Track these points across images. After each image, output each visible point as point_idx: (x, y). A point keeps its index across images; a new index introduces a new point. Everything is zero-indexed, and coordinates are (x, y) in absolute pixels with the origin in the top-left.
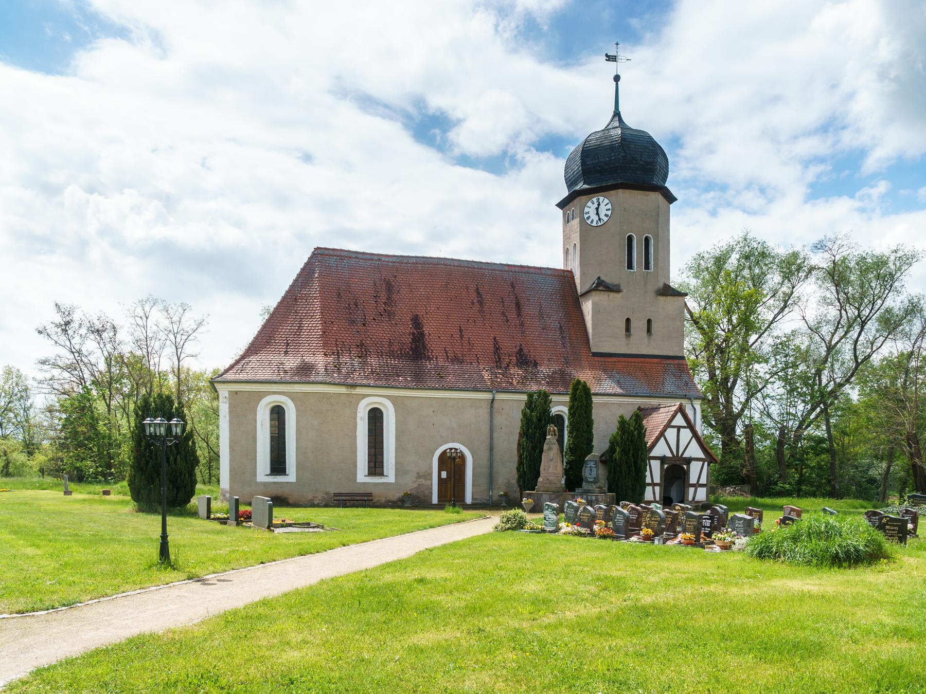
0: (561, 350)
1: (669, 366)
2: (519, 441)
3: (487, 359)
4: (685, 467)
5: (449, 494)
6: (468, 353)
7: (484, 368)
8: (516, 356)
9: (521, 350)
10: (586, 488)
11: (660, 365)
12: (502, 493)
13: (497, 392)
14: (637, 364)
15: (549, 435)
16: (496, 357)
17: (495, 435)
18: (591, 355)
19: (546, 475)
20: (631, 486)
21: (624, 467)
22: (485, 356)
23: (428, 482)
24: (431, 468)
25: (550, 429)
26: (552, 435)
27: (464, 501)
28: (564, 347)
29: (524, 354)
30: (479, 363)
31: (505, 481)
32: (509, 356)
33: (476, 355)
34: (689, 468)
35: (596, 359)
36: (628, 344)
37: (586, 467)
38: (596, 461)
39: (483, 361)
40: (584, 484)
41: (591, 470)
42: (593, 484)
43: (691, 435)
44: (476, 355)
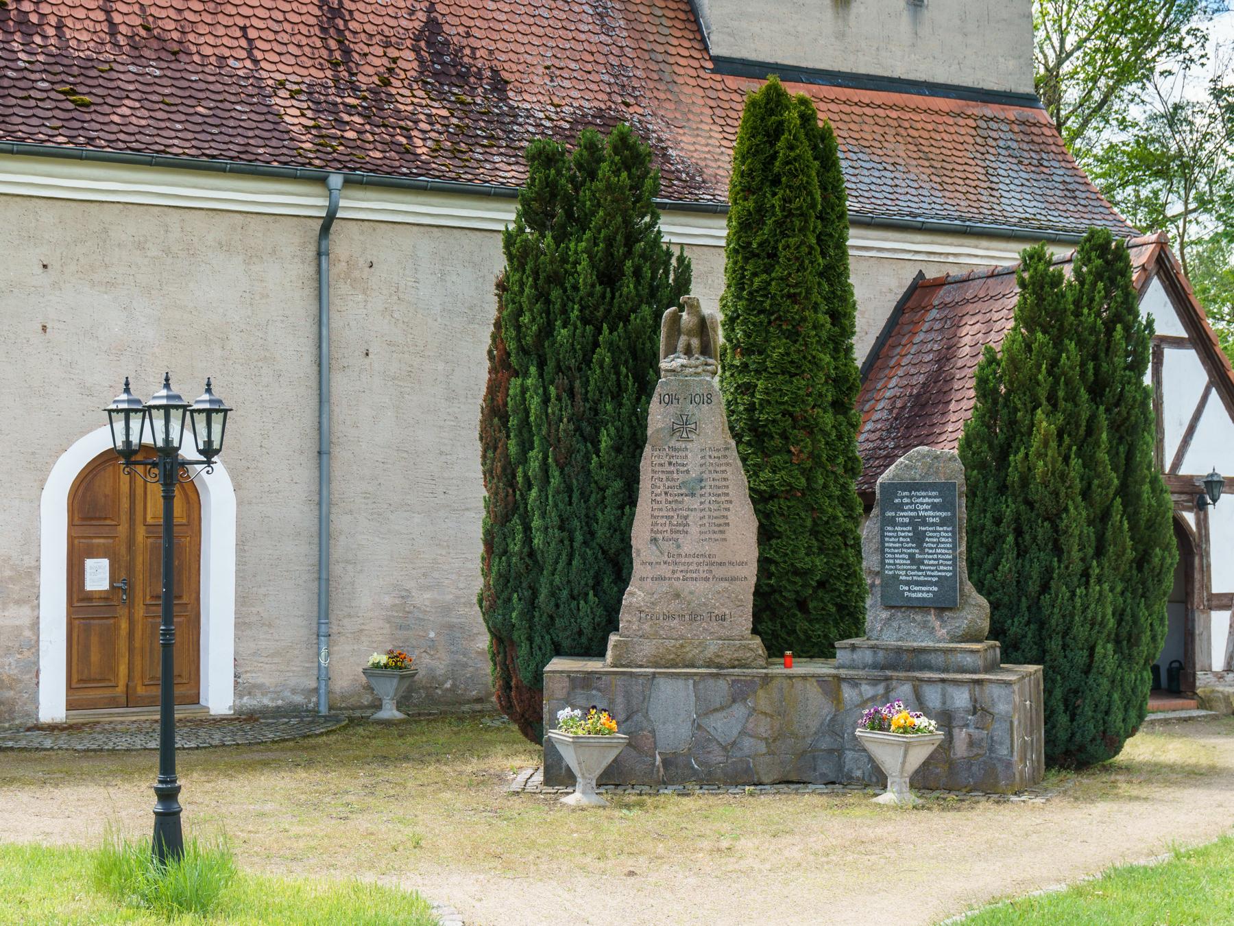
0: (594, 39)
1: (993, 125)
2: (494, 389)
3: (292, 49)
4: (1190, 518)
5: (123, 669)
6: (208, 18)
7: (282, 84)
8: (416, 50)
9: (433, 25)
10: (890, 639)
11: (961, 121)
12: (383, 659)
13: (348, 182)
14: (881, 112)
15: (671, 350)
16: (333, 44)
17: (340, 384)
18: (709, 65)
19: (665, 570)
20: (1111, 623)
21: (1077, 519)
22: (284, 38)
23: (17, 616)
24: (31, 540)
25: (676, 319)
26: (688, 352)
27: (199, 703)
28: (607, 30)
29: (446, 43)
30: (256, 61)
31: (388, 600)
32: (387, 45)
33: (244, 29)
34: (1203, 523)
35: (732, 82)
36: (841, 36)
37: (892, 522)
38: (945, 489)
39: (273, 57)
40: (874, 614)
41: (919, 539)
42: (932, 618)
43: (1201, 376)
44: (244, 29)
